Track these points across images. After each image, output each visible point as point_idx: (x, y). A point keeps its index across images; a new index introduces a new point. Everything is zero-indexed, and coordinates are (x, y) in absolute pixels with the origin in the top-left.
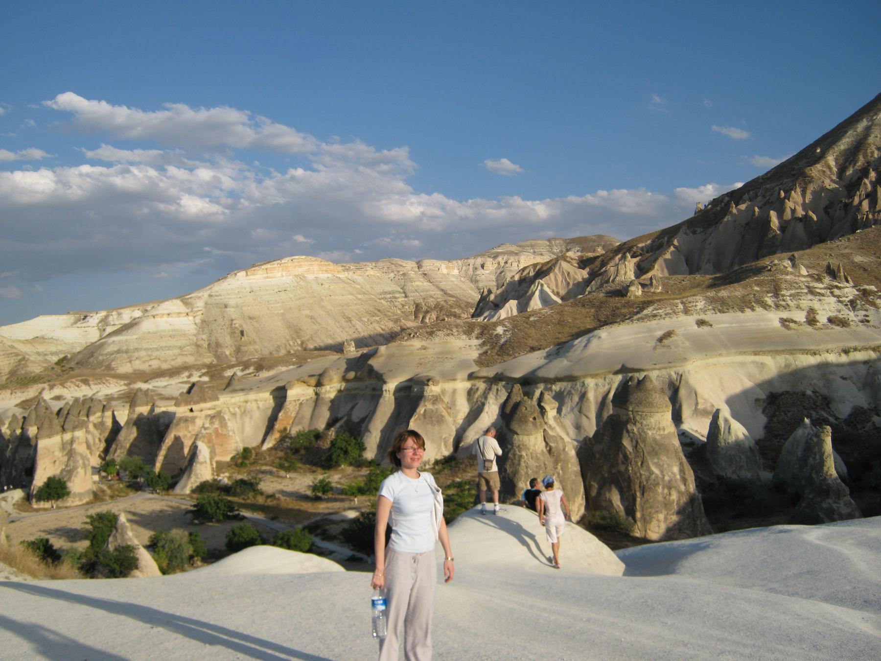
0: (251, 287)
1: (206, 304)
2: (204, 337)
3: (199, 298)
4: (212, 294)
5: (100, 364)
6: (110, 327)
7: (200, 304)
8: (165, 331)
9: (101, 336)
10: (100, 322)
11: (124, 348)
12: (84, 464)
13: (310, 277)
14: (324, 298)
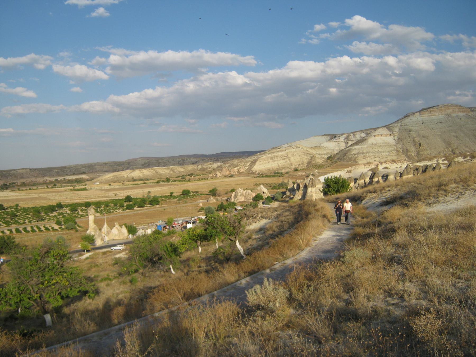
0: (422, 121)
2: (400, 146)
3: (396, 126)
5: (350, 159)
7: (397, 130)
8: (380, 143)
9: (346, 146)
10: (345, 139)
11: (361, 152)
13: (454, 115)
14: (462, 126)
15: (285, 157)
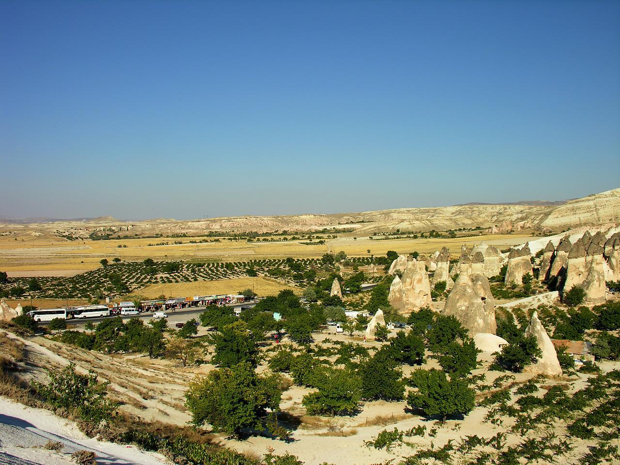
12: (599, 278)
15: (591, 209)
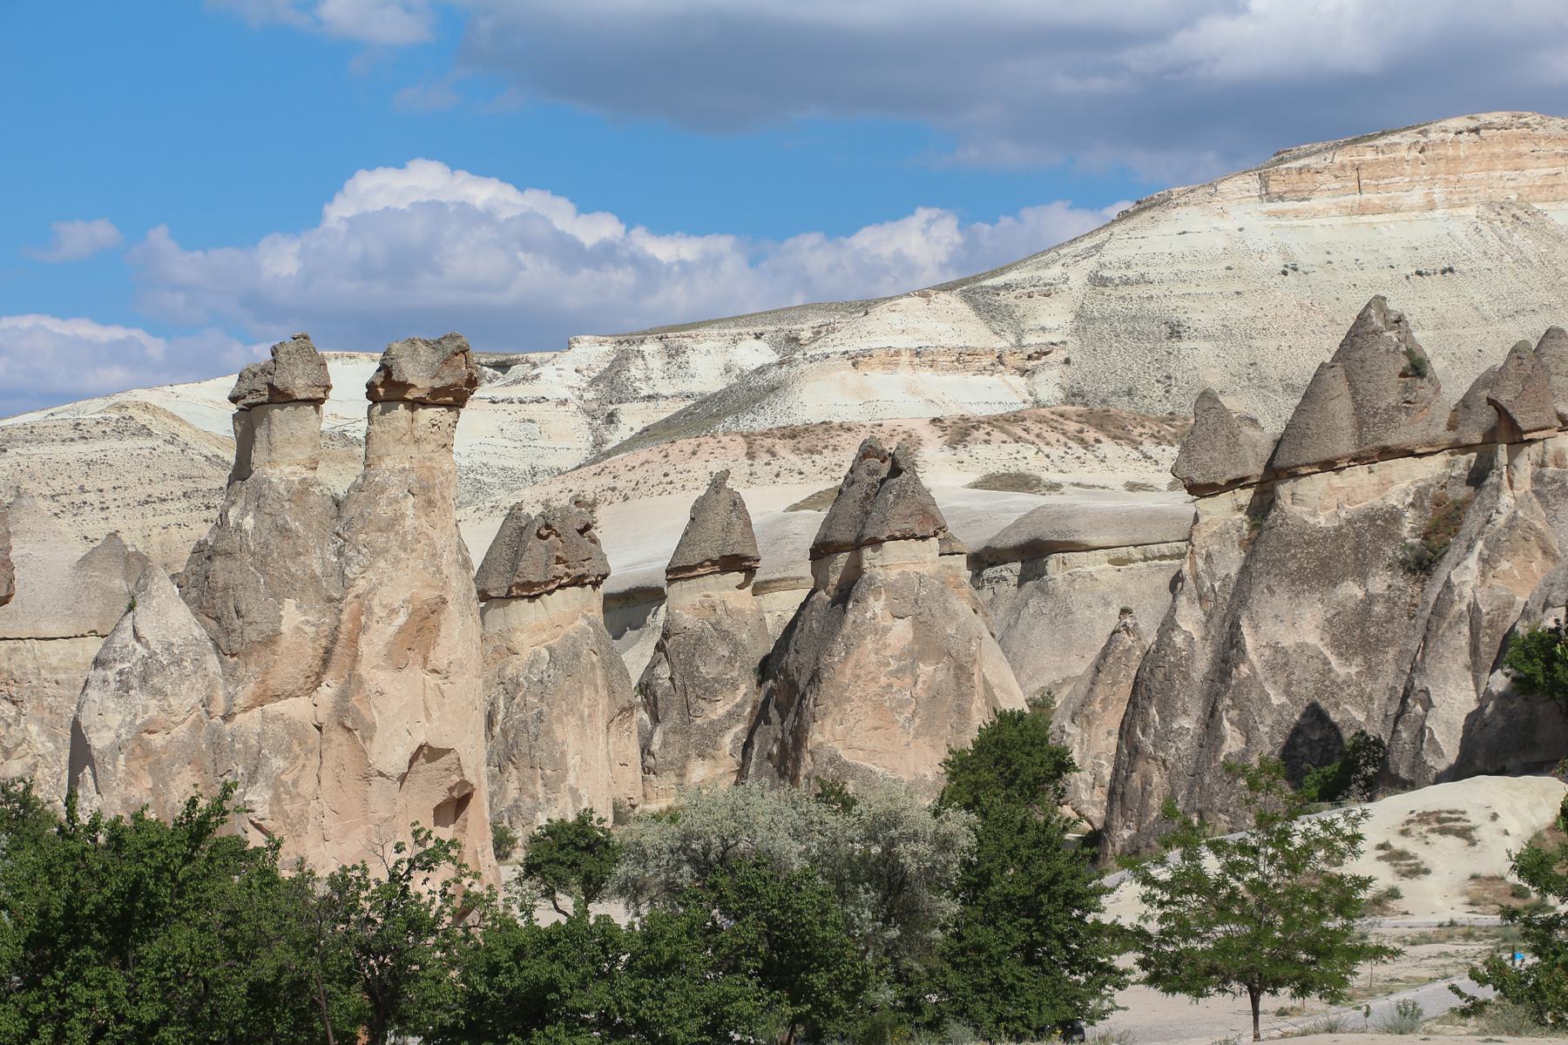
0: (1284, 251)
1: (1083, 318)
4: (1106, 273)
6: (638, 406)
9: (598, 443)
